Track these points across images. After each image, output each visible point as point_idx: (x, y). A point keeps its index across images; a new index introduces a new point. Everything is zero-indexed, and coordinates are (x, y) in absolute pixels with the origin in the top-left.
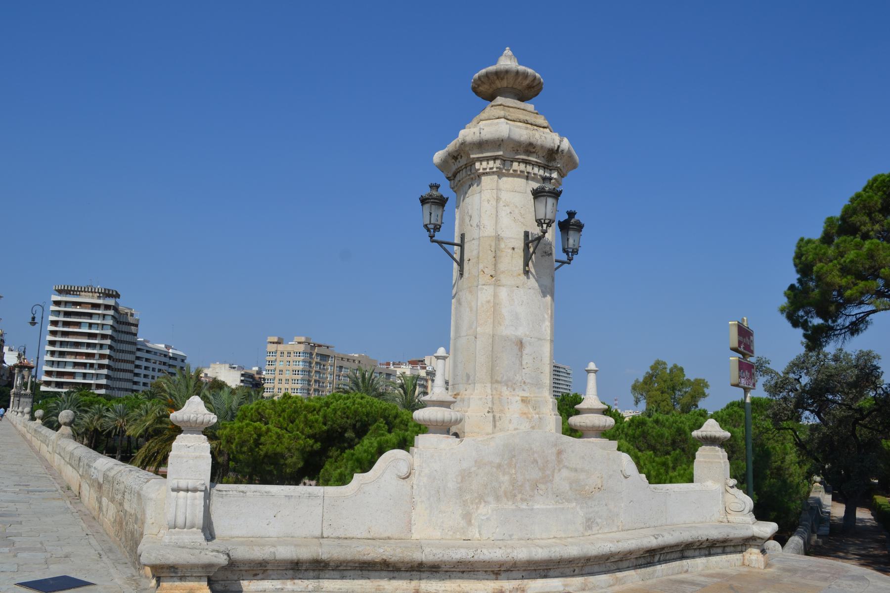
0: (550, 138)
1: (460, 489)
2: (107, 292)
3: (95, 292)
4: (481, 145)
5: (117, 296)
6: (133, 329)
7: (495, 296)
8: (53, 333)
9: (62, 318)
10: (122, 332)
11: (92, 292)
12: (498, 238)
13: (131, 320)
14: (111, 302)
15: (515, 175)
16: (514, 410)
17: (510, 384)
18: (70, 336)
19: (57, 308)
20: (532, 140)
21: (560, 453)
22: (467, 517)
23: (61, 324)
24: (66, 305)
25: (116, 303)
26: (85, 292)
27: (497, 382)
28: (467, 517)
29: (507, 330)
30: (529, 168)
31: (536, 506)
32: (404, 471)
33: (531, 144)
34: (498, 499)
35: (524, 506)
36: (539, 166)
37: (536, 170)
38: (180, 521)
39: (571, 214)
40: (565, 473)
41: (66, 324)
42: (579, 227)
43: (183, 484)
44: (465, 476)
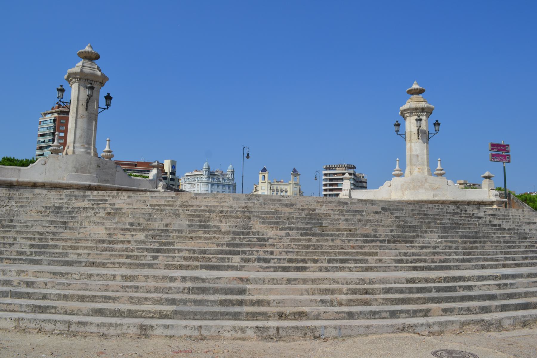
0: (423, 105)
1: (401, 188)
2: (349, 166)
3: (343, 167)
4: (405, 110)
5: (354, 168)
6: (364, 184)
7: (411, 145)
8: (325, 190)
9: (329, 182)
10: (359, 186)
11: (342, 167)
12: (411, 132)
13: (363, 180)
14: (351, 171)
15: (414, 116)
16: (416, 171)
17: (416, 165)
18: (333, 191)
19: (326, 177)
20: (417, 107)
21: (426, 179)
22: (403, 194)
23: (328, 185)
24: (330, 175)
25: (354, 171)
26: (338, 167)
27: (412, 165)
28: (403, 194)
29: (414, 153)
30: (418, 113)
31: (420, 191)
32: (389, 185)
33: (416, 108)
34: (410, 189)
35: (417, 191)
36: (420, 112)
37: (420, 113)
38: (345, 195)
39: (437, 121)
40: (428, 184)
41: (331, 185)
42: (439, 124)
43: (345, 189)
44: (402, 185)
